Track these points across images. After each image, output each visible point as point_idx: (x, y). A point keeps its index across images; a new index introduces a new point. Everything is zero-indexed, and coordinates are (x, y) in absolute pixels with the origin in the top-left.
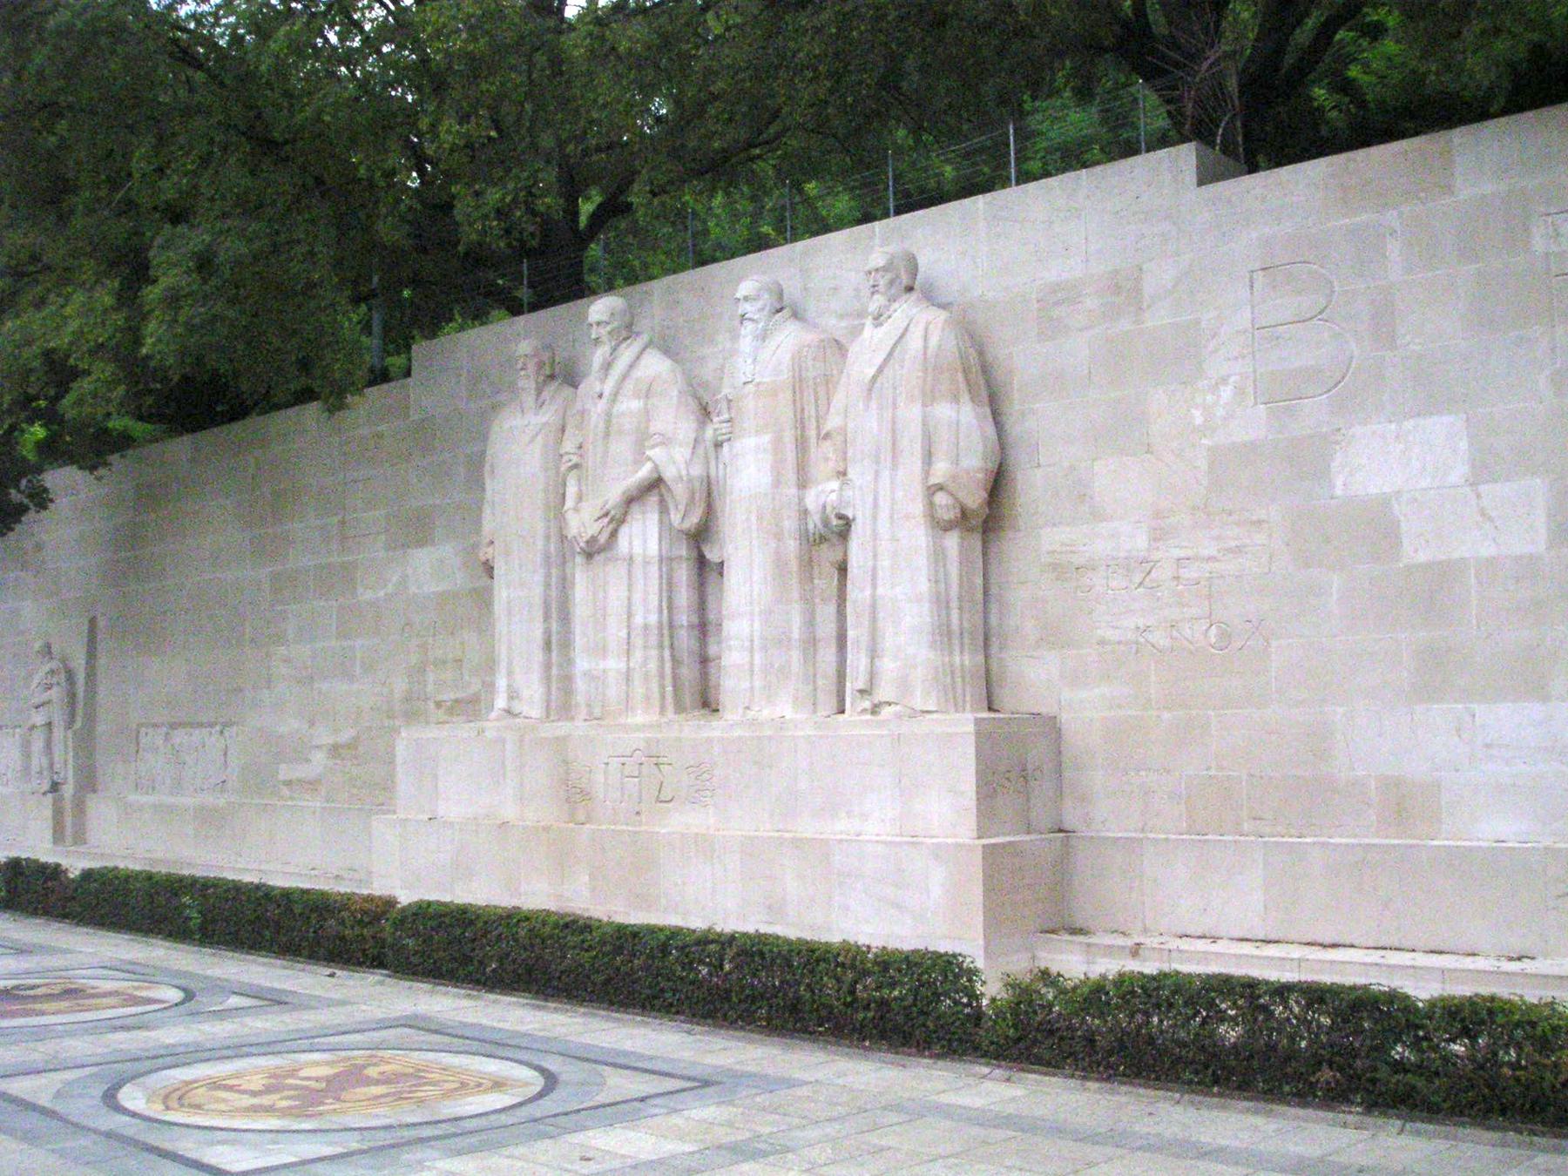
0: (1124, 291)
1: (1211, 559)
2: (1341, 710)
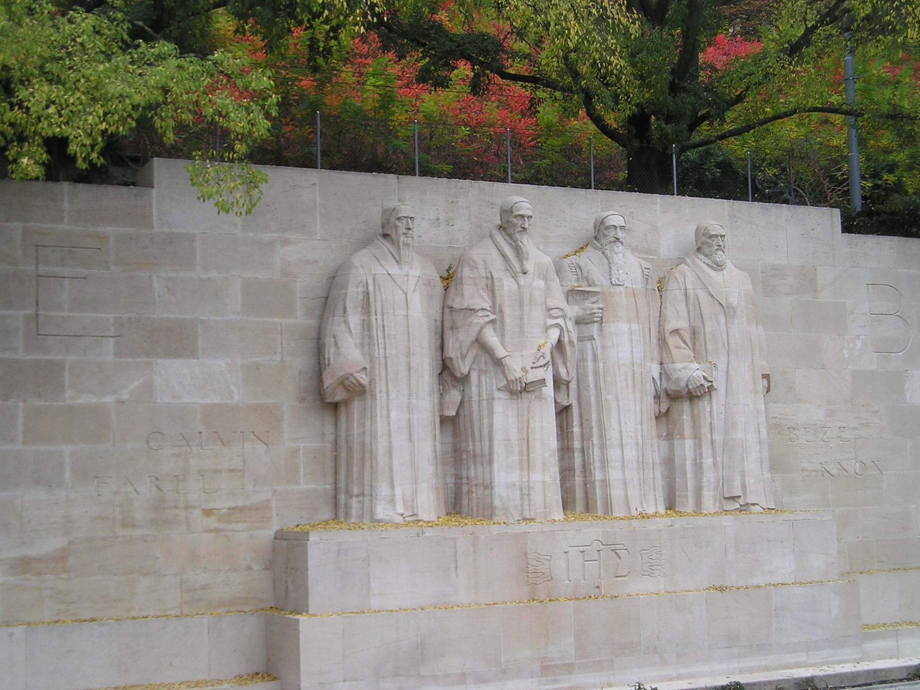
0: (807, 280)
1: (855, 428)
2: (913, 506)
